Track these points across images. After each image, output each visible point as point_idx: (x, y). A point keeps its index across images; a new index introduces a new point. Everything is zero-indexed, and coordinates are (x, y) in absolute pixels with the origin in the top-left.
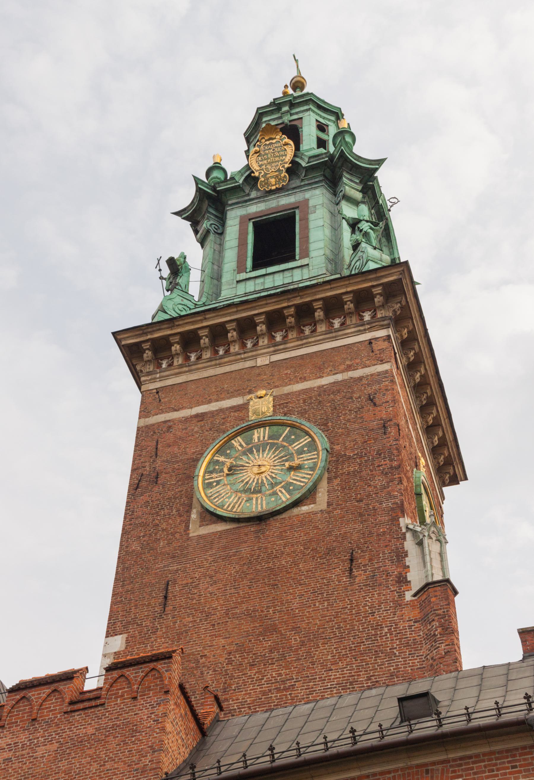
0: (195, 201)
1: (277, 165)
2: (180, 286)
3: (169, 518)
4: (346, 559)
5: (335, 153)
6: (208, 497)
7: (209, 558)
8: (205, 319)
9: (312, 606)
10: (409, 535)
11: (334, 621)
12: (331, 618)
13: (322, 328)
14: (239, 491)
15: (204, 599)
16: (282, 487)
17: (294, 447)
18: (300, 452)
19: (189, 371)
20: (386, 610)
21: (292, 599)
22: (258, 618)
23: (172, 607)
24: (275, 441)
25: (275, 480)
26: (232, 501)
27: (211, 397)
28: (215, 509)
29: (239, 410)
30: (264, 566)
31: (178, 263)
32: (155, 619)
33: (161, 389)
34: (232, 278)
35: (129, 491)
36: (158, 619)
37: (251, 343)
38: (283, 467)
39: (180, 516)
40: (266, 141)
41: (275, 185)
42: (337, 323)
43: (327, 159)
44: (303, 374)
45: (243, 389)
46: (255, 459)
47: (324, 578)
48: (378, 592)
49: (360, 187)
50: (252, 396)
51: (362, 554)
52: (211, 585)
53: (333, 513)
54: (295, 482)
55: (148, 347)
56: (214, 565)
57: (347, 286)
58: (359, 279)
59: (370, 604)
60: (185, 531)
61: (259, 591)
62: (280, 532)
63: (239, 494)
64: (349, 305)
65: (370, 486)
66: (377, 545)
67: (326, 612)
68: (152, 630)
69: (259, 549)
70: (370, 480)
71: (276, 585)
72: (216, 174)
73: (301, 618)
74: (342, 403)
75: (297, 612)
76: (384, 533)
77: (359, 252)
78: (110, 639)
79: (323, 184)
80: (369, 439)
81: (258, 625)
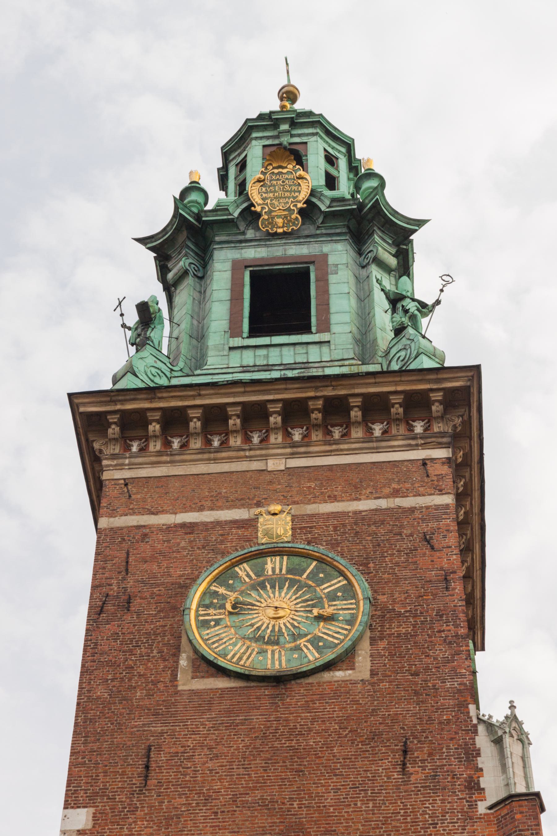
0: (168, 229)
1: (287, 203)
2: (152, 342)
3: (148, 660)
4: (397, 749)
5: (367, 201)
6: (205, 640)
7: (207, 723)
8: (200, 395)
9: (353, 806)
10: (481, 729)
11: (382, 828)
12: (378, 824)
13: (357, 433)
14: (248, 638)
15: (201, 777)
16: (308, 641)
17: (324, 589)
18: (332, 597)
19: (171, 462)
20: (452, 823)
21: (324, 793)
22: (277, 812)
23: (156, 781)
24: (297, 578)
25: (297, 630)
26: (238, 651)
27: (203, 503)
28: (216, 658)
29: (243, 527)
30: (285, 744)
31: (151, 310)
32: (133, 794)
33: (131, 481)
34: (222, 342)
35: (89, 616)
36: (137, 794)
37: (259, 437)
38: (309, 615)
39: (165, 660)
40: (274, 168)
41: (283, 227)
42: (378, 429)
43: (355, 207)
44: (332, 491)
45: (249, 498)
46: (270, 597)
47: (368, 771)
48: (441, 797)
49: (393, 251)
50: (263, 510)
51: (419, 745)
52: (211, 760)
53: (379, 685)
54: (325, 637)
55: (116, 420)
56: (214, 734)
57: (396, 383)
58: (414, 378)
59: (430, 812)
60: (171, 681)
61: (277, 776)
62: (305, 701)
63: (248, 643)
64: (397, 409)
65: (428, 656)
66: (439, 736)
67: (371, 816)
68: (129, 808)
69: (277, 719)
70: (428, 648)
71: (302, 771)
72: (194, 196)
73: (338, 820)
74: (387, 540)
75: (332, 810)
76: (449, 721)
77: (404, 339)
78: (70, 811)
79: (348, 238)
80: (426, 594)
81: (278, 821)
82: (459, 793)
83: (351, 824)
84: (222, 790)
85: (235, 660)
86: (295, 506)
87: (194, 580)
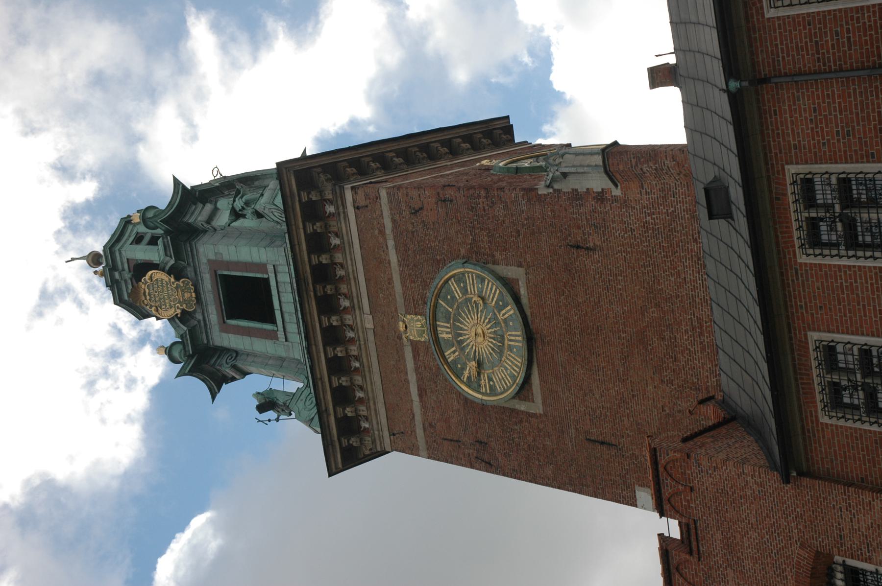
0: (202, 378)
2: (287, 401)
5: (163, 228)
6: (505, 391)
8: (321, 379)
9: (621, 292)
11: (637, 271)
13: (339, 257)
17: (459, 296)
18: (465, 291)
21: (613, 313)
22: (630, 350)
28: (517, 385)
31: (263, 401)
32: (623, 456)
35: (493, 473)
36: (623, 452)
37: (349, 332)
40: (146, 299)
41: (191, 293)
42: (335, 241)
43: (169, 238)
45: (396, 345)
46: (468, 338)
47: (594, 277)
48: (611, 223)
49: (200, 205)
50: (404, 337)
51: (572, 236)
54: (495, 299)
55: (346, 441)
57: (297, 228)
63: (504, 358)
65: (504, 222)
70: (497, 221)
71: (598, 328)
72: (176, 354)
73: (633, 304)
74: (418, 243)
75: (626, 308)
76: (553, 211)
78: (638, 503)
79: (194, 243)
81: (636, 350)
82: (607, 208)
83: (635, 295)
84: (616, 389)
85: (518, 370)
86: (399, 311)
87: (460, 394)
